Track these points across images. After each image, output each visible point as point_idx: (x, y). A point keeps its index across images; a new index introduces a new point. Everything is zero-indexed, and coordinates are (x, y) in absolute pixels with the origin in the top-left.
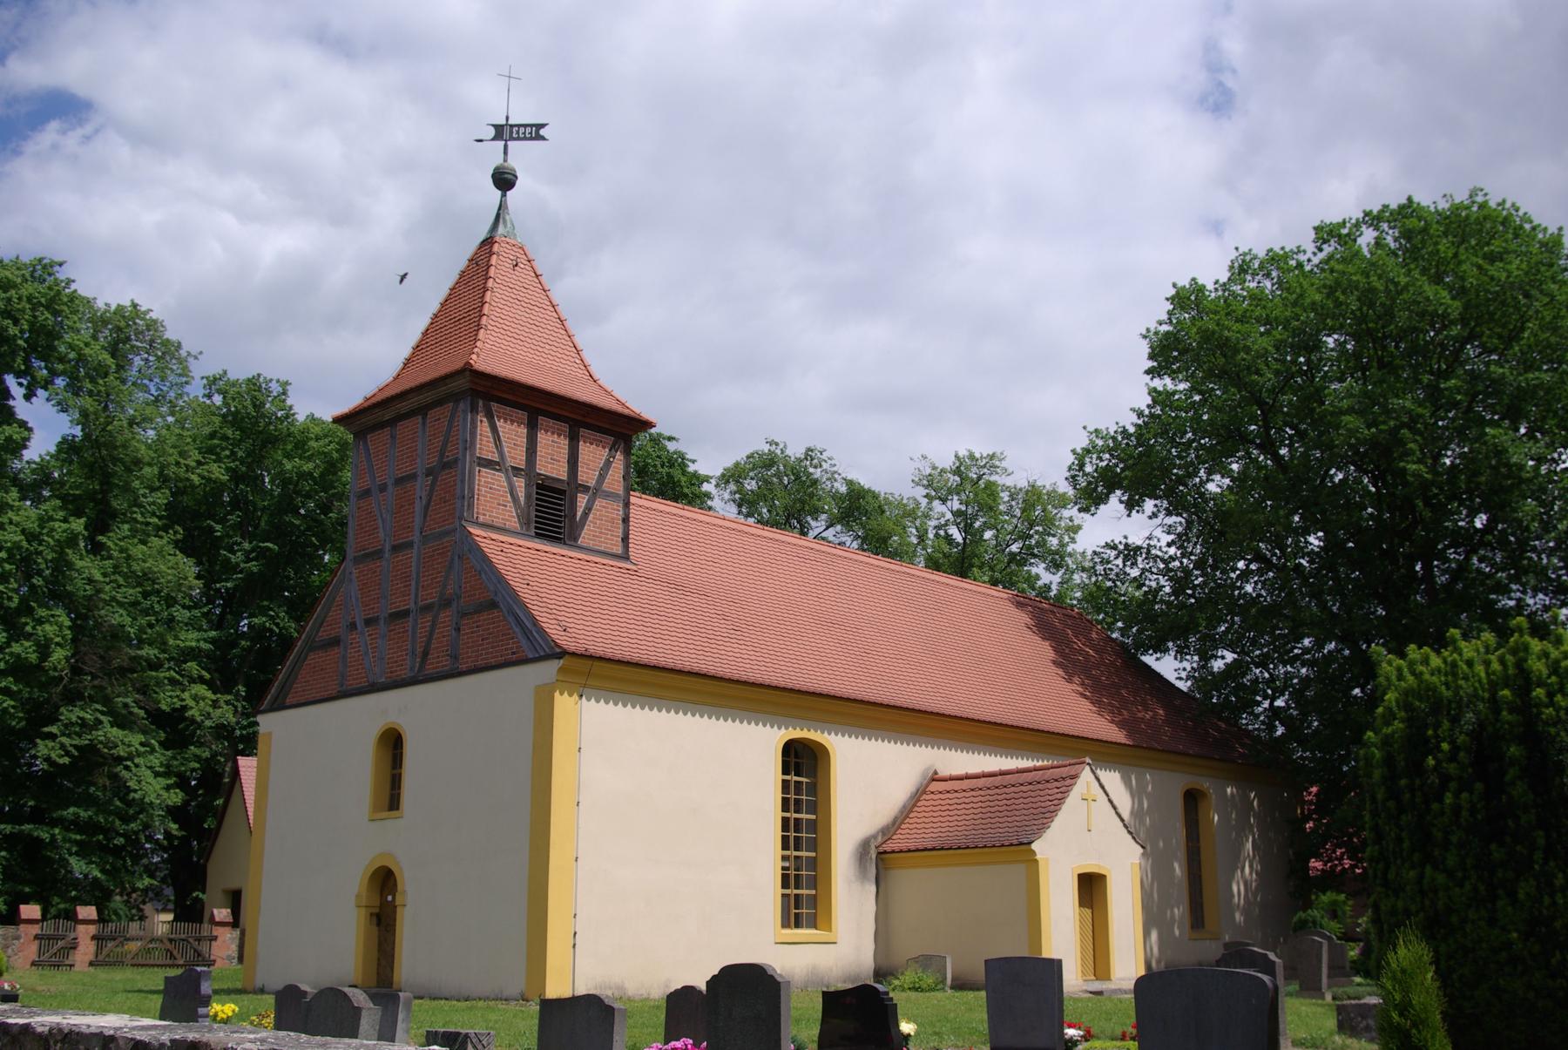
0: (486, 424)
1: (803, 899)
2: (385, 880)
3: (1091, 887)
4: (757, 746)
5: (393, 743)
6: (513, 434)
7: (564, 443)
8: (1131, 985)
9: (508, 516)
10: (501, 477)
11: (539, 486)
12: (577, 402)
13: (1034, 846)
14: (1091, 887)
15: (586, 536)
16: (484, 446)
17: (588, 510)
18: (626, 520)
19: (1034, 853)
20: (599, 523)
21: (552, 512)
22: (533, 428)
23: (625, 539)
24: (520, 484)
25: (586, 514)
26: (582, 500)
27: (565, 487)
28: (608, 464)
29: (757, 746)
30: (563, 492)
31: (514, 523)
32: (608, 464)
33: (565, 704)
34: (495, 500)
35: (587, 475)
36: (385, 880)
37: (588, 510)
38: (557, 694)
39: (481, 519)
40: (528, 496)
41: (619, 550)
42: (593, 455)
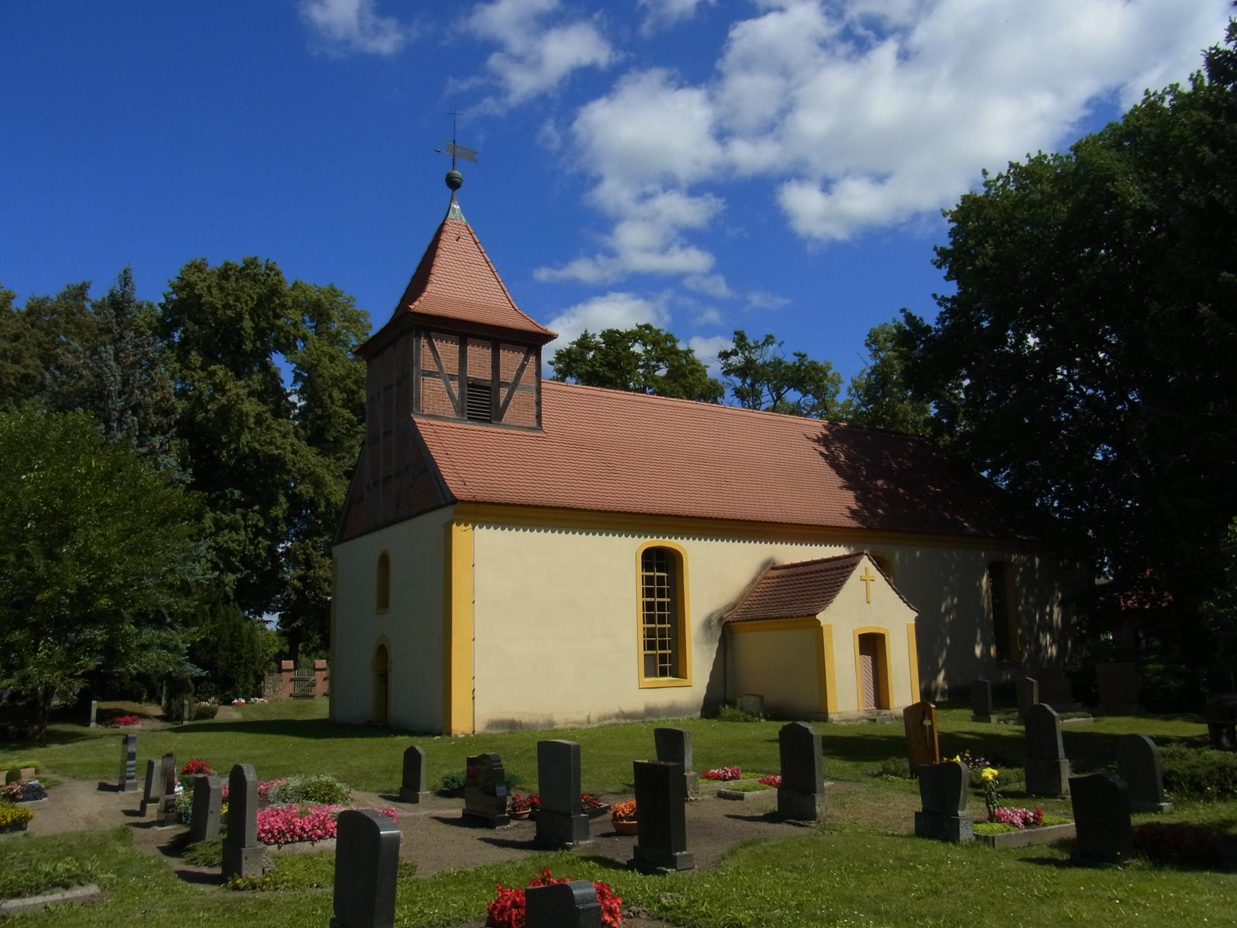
0: (427, 347)
1: (663, 654)
2: (382, 652)
3: (872, 644)
4: (624, 552)
5: (384, 560)
6: (448, 350)
7: (488, 353)
8: (901, 712)
9: (448, 408)
10: (440, 382)
11: (469, 385)
12: (494, 326)
13: (818, 617)
14: (872, 644)
15: (508, 417)
16: (425, 359)
17: (509, 396)
18: (539, 403)
19: (819, 622)
20: (518, 409)
21: (482, 403)
22: (463, 345)
23: (539, 417)
24: (455, 385)
25: (507, 402)
26: (504, 392)
27: (489, 384)
28: (523, 367)
29: (624, 552)
30: (488, 388)
31: (451, 413)
32: (523, 367)
33: (460, 533)
34: (435, 398)
35: (507, 374)
36: (382, 652)
37: (509, 396)
38: (454, 526)
39: (426, 412)
40: (461, 394)
41: (534, 424)
42: (511, 360)
